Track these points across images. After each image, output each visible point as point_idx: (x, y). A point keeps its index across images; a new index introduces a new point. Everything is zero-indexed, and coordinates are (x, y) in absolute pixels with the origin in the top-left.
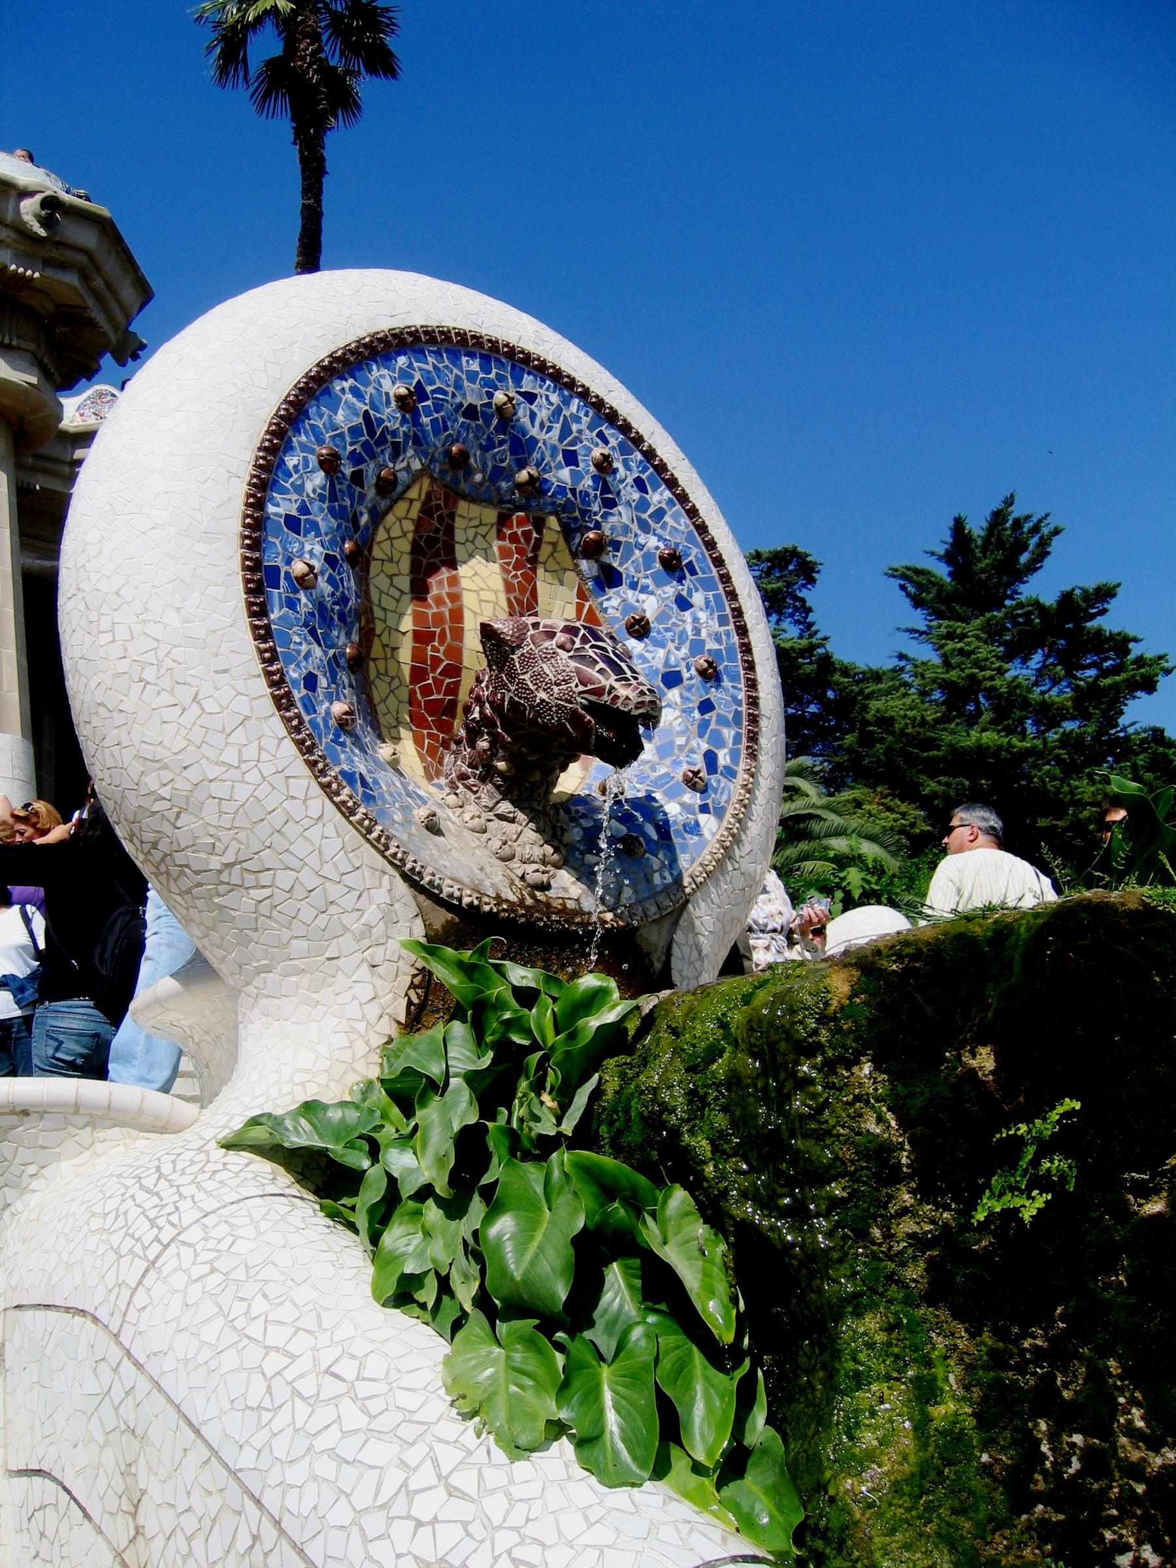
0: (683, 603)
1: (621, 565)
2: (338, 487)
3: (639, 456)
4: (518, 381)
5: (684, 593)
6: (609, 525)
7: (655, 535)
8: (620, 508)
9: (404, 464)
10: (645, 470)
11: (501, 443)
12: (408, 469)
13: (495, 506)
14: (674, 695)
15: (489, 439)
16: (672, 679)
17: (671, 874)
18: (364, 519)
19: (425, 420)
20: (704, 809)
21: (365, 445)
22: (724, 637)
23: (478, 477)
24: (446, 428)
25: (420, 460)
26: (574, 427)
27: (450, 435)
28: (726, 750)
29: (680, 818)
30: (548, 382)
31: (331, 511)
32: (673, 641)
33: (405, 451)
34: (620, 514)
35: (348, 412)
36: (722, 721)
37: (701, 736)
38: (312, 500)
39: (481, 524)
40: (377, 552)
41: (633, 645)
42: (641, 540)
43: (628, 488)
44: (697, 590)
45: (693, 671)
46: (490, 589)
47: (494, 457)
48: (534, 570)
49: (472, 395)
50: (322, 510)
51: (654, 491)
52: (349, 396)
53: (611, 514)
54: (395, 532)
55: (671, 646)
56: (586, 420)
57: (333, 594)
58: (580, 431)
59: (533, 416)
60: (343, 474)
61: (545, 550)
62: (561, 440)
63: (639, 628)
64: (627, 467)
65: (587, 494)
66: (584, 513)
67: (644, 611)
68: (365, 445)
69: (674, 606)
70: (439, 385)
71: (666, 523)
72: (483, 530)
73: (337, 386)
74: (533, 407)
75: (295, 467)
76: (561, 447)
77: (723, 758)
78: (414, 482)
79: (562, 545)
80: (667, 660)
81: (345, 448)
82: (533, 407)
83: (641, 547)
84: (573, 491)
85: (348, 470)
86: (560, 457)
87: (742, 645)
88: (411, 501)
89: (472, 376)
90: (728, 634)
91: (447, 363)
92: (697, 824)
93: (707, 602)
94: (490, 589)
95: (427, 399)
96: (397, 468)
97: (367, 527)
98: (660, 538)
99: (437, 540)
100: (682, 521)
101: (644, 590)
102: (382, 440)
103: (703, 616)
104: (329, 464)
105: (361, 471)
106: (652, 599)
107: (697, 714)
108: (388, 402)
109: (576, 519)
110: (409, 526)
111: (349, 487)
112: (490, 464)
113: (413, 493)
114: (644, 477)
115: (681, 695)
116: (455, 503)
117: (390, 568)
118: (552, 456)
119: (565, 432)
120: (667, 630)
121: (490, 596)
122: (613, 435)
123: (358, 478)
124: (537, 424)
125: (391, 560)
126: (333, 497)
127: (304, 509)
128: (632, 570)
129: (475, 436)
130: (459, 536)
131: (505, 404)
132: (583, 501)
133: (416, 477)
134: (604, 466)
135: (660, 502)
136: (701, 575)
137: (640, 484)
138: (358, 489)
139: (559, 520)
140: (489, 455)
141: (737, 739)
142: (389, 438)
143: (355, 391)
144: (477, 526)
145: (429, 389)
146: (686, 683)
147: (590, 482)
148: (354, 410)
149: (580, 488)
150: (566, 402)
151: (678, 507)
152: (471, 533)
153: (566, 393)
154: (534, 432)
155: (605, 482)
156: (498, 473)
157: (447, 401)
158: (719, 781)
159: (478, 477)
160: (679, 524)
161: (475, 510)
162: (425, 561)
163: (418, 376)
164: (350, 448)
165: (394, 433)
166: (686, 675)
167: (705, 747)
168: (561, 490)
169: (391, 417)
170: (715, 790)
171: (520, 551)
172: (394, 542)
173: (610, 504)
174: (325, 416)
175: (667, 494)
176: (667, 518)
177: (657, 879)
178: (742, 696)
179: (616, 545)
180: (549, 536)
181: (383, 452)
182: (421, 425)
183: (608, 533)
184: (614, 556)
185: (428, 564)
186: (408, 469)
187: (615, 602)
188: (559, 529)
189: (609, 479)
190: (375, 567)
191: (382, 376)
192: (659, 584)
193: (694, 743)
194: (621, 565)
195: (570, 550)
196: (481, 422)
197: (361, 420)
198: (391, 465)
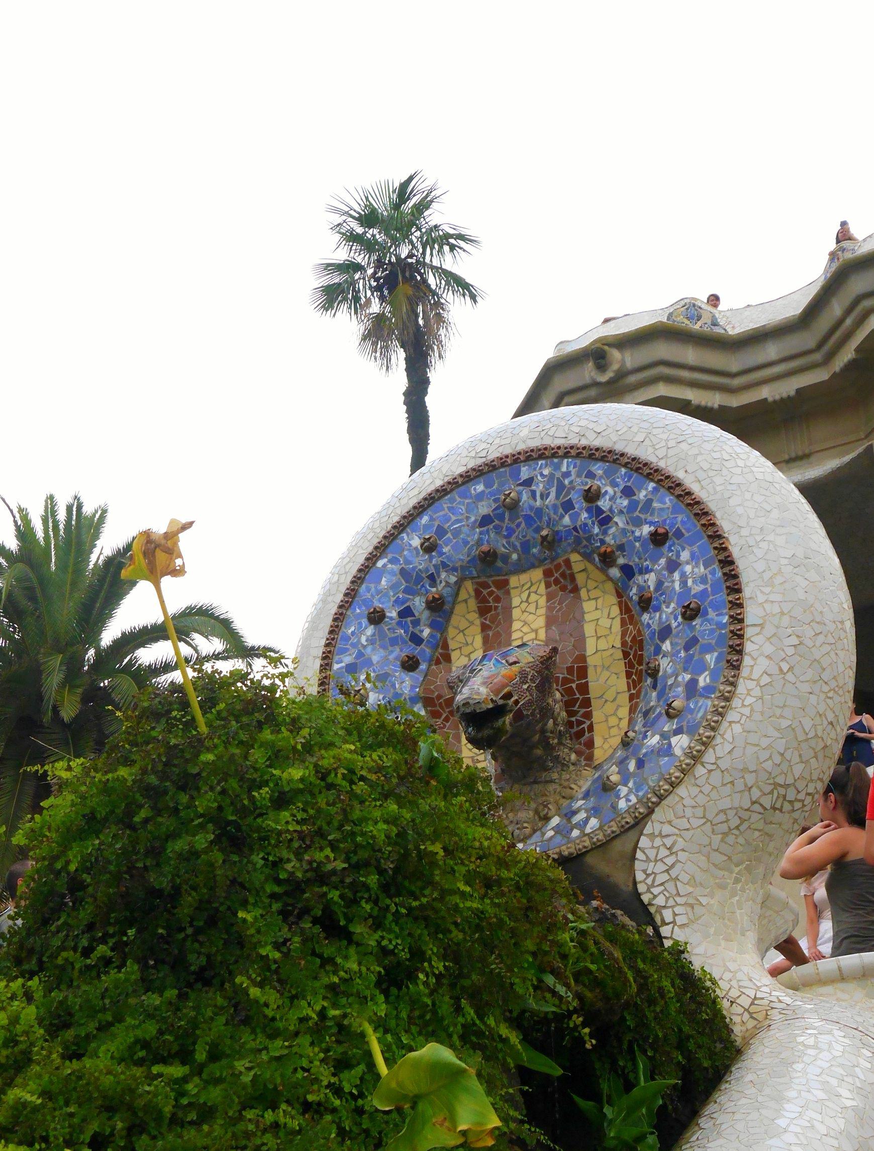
0: (673, 565)
1: (630, 560)
2: (386, 628)
3: (623, 470)
4: (516, 475)
5: (674, 558)
6: (611, 537)
7: (647, 523)
8: (616, 519)
9: (443, 584)
10: (629, 480)
11: (518, 526)
12: (448, 584)
13: (538, 567)
14: (667, 646)
15: (508, 529)
16: (665, 632)
17: (637, 796)
18: (426, 632)
19: (445, 550)
20: (678, 732)
21: (405, 591)
22: (709, 576)
23: (515, 556)
24: (466, 543)
25: (454, 575)
26: (566, 482)
27: (473, 545)
28: (707, 673)
29: (657, 746)
30: (540, 463)
31: (384, 647)
32: (664, 602)
33: (439, 576)
34: (616, 523)
35: (388, 577)
36: (708, 649)
37: (685, 670)
38: (364, 647)
39: (532, 585)
40: (452, 645)
41: (646, 617)
42: (637, 534)
43: (618, 501)
44: (683, 549)
45: (680, 619)
46: (533, 631)
47: (517, 537)
48: (579, 598)
49: (484, 508)
50: (373, 649)
51: (640, 491)
52: (390, 566)
53: (610, 528)
54: (463, 624)
55: (664, 607)
56: (574, 472)
57: (383, 699)
58: (571, 482)
59: (533, 493)
60: (391, 618)
61: (580, 579)
62: (557, 497)
63: (646, 603)
64: (614, 484)
65: (586, 525)
66: (590, 538)
67: (649, 587)
68: (405, 591)
69: (665, 573)
70: (454, 518)
71: (654, 509)
72: (533, 589)
73: (380, 564)
74: (533, 488)
75: (353, 633)
76: (558, 503)
77: (703, 680)
78: (459, 590)
79: (590, 567)
80: (660, 618)
81: (390, 600)
82: (533, 488)
83: (638, 539)
84: (575, 529)
85: (394, 614)
86: (561, 510)
87: (725, 574)
88: (466, 601)
89: (480, 497)
90: (713, 573)
91: (458, 499)
92: (670, 745)
93: (693, 556)
94: (533, 631)
95: (446, 532)
96: (440, 588)
97: (431, 636)
98: (651, 523)
99: (498, 614)
100: (667, 500)
101: (648, 571)
102: (419, 579)
103: (688, 569)
104: (376, 618)
105: (408, 608)
106: (653, 574)
107: (683, 654)
108: (418, 553)
109: (586, 546)
110: (474, 616)
111: (399, 624)
112: (518, 544)
113: (463, 595)
114: (629, 484)
115: (672, 644)
116: (507, 582)
117: (466, 650)
118: (555, 514)
119: (561, 487)
120: (661, 595)
121: (533, 635)
122: (599, 469)
123: (406, 613)
124: (538, 498)
125: (467, 644)
126: (382, 635)
127: (360, 655)
128: (637, 560)
129: (496, 533)
130: (516, 601)
131: (505, 500)
132: (584, 531)
133: (459, 584)
134: (591, 496)
135: (645, 496)
136: (687, 535)
137: (628, 492)
138: (409, 619)
139: (579, 553)
140: (513, 539)
141: (718, 660)
142: (424, 575)
143: (393, 561)
144: (529, 588)
145: (446, 526)
146: (674, 632)
147: (585, 515)
148: (392, 573)
149: (579, 523)
150: (558, 467)
151: (662, 490)
152: (524, 596)
153: (556, 460)
154: (538, 503)
155: (598, 508)
156: (526, 546)
157: (464, 526)
158: (697, 703)
159: (515, 556)
160: (665, 503)
161: (524, 577)
162: (491, 633)
163: (436, 523)
164: (393, 599)
165: (427, 570)
166: (674, 625)
167: (688, 677)
168: (569, 532)
169: (421, 562)
170: (691, 711)
171: (563, 589)
172: (465, 632)
173: (605, 521)
174: (373, 589)
175: (652, 485)
176: (655, 505)
177: (622, 804)
178: (725, 619)
179: (621, 547)
180: (576, 567)
181: (423, 586)
182: (445, 553)
183: (612, 542)
184: (624, 556)
185: (493, 635)
186: (448, 584)
187: (634, 590)
188: (580, 558)
189: (600, 503)
190: (454, 655)
191: (413, 538)
192: (655, 560)
193: (680, 679)
194: (630, 560)
195: (597, 568)
196: (497, 522)
197: (399, 576)
198: (434, 590)
